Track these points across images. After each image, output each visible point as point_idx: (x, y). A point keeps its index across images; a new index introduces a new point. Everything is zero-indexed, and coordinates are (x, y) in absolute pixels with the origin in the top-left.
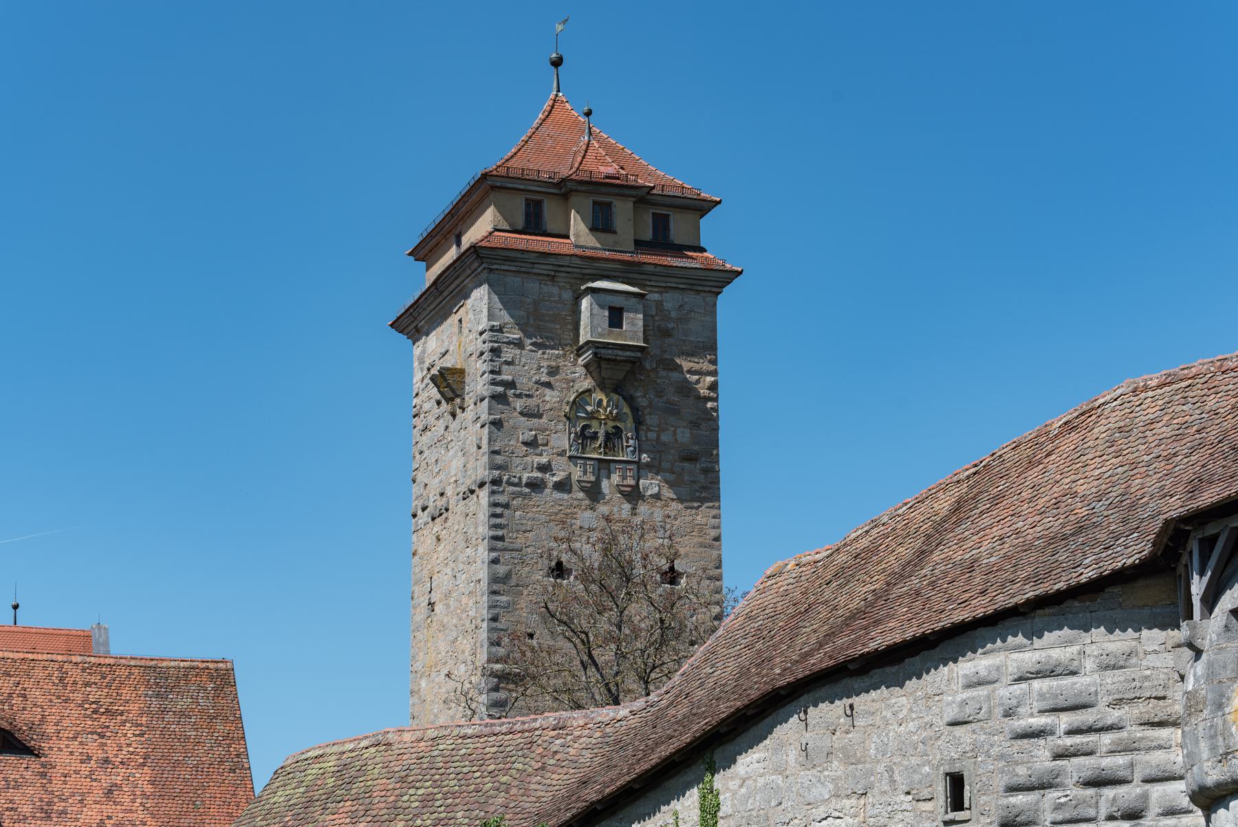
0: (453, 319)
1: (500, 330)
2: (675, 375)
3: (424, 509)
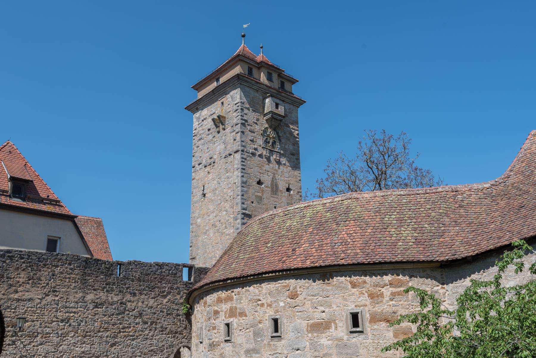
0: (219, 103)
1: (243, 103)
2: (288, 129)
3: (199, 164)
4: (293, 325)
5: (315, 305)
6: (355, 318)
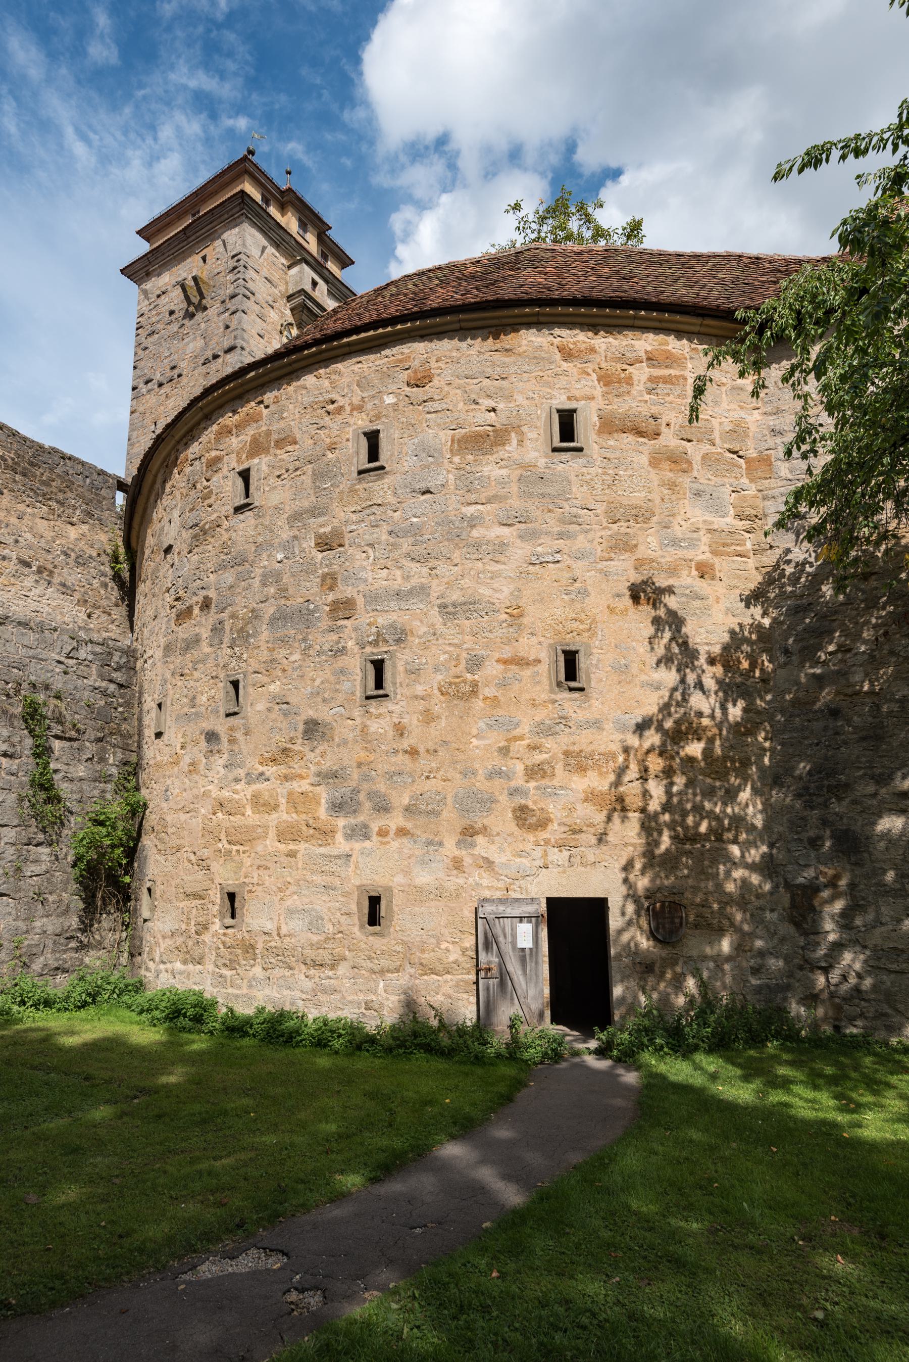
4: (416, 441)
5: (473, 396)
6: (567, 423)
